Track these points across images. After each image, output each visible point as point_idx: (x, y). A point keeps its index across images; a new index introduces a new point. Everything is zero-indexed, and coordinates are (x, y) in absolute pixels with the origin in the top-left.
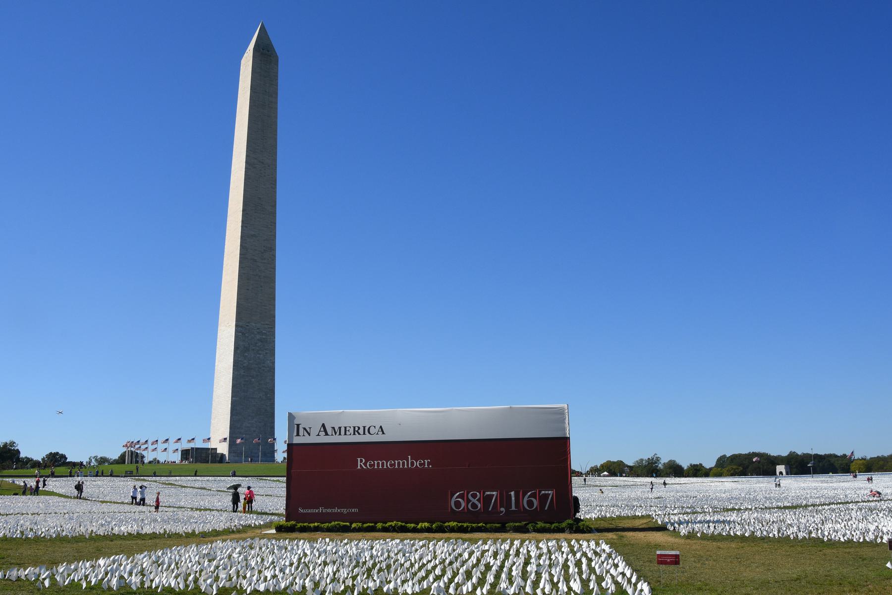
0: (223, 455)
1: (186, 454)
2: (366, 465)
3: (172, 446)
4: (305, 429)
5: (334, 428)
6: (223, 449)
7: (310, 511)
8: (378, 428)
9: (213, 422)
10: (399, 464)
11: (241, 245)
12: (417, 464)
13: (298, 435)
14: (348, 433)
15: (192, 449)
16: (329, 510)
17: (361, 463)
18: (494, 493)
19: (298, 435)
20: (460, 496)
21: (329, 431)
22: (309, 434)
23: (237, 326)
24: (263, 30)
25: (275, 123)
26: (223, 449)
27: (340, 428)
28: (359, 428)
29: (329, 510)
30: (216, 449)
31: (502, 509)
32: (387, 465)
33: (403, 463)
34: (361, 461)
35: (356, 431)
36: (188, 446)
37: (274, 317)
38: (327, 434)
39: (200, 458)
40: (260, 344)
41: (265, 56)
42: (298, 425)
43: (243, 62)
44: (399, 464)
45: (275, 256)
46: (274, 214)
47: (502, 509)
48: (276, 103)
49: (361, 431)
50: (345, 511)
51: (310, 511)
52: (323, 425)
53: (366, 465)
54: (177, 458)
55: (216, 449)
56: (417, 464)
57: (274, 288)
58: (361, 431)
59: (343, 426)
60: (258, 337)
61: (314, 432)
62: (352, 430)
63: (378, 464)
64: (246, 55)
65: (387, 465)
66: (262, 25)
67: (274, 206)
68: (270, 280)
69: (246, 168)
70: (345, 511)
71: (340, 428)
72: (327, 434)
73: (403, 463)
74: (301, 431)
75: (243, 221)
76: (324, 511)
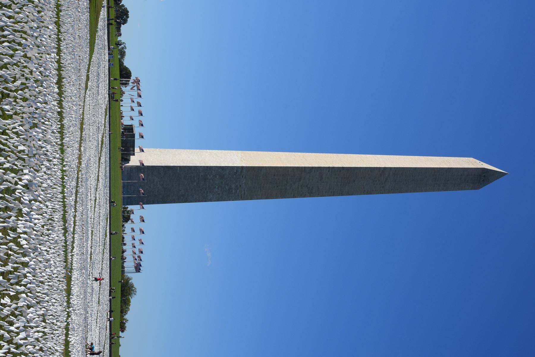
0: (128, 160)
1: (129, 129)
3: (135, 123)
6: (134, 161)
9: (158, 150)
11: (312, 167)
15: (133, 136)
23: (242, 167)
24: (501, 175)
25: (421, 191)
26: (134, 161)
30: (134, 155)
36: (137, 131)
37: (251, 199)
39: (124, 141)
40: (227, 188)
41: (478, 179)
43: (472, 159)
45: (305, 196)
46: (341, 194)
48: (439, 190)
54: (126, 121)
55: (134, 155)
57: (276, 197)
60: (233, 186)
64: (478, 161)
66: (505, 174)
67: (348, 194)
68: (283, 194)
69: (380, 168)
75: (334, 167)
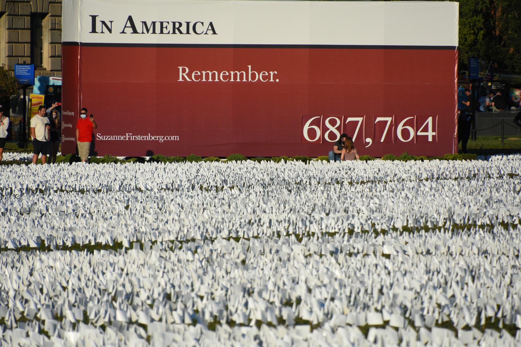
2: (190, 78)
4: (103, 23)
5: (145, 23)
7: (112, 138)
8: (206, 24)
10: (235, 76)
12: (259, 77)
13: (94, 31)
14: (165, 31)
16: (139, 138)
17: (183, 74)
18: (360, 119)
19: (94, 31)
20: (316, 123)
21: (139, 27)
22: (110, 31)
27: (154, 23)
28: (180, 24)
29: (139, 138)
31: (369, 140)
32: (220, 77)
33: (241, 75)
34: (184, 71)
35: (176, 28)
38: (135, 31)
42: (94, 18)
44: (235, 76)
47: (369, 140)
49: (184, 29)
50: (161, 139)
51: (112, 138)
52: (130, 19)
53: (190, 78)
56: (259, 77)
58: (184, 29)
59: (158, 20)
61: (117, 27)
62: (170, 27)
63: (207, 75)
65: (220, 77)
70: (161, 139)
71: (154, 23)
72: (135, 31)
73: (241, 75)
74: (99, 25)
76: (133, 138)
